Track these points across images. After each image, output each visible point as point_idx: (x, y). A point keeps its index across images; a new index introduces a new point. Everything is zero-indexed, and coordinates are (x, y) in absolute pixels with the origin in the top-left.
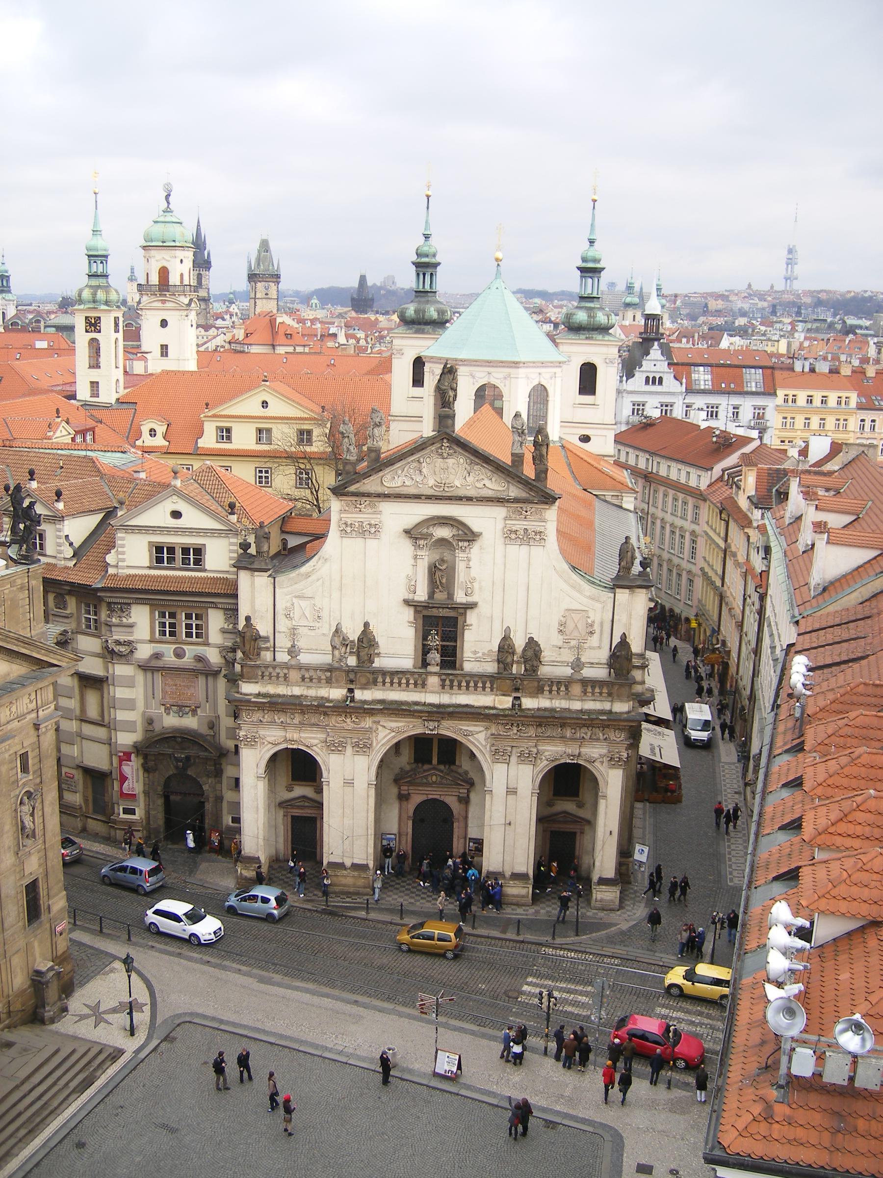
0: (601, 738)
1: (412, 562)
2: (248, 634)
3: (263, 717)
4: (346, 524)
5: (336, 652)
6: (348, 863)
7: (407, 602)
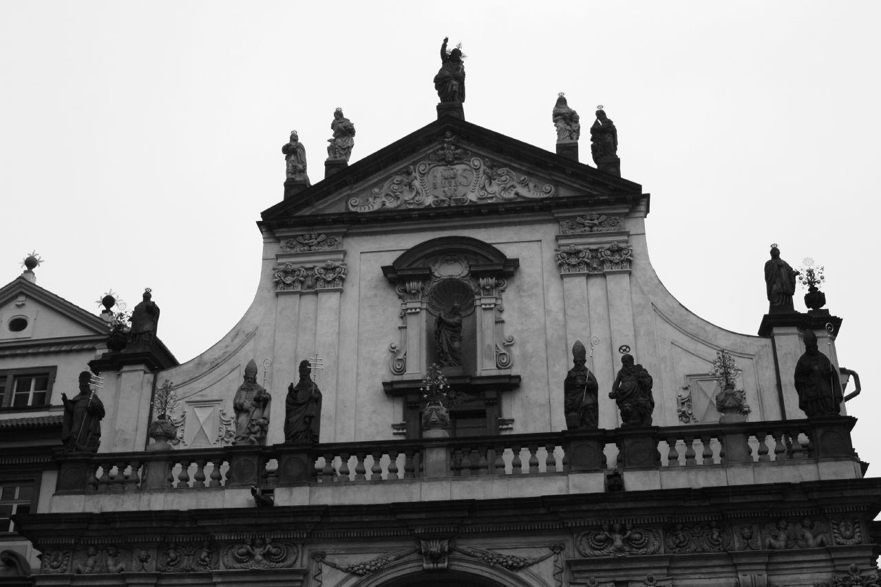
0: (811, 542)
3: (85, 565)
4: (286, 273)
5: (243, 419)
7: (392, 391)
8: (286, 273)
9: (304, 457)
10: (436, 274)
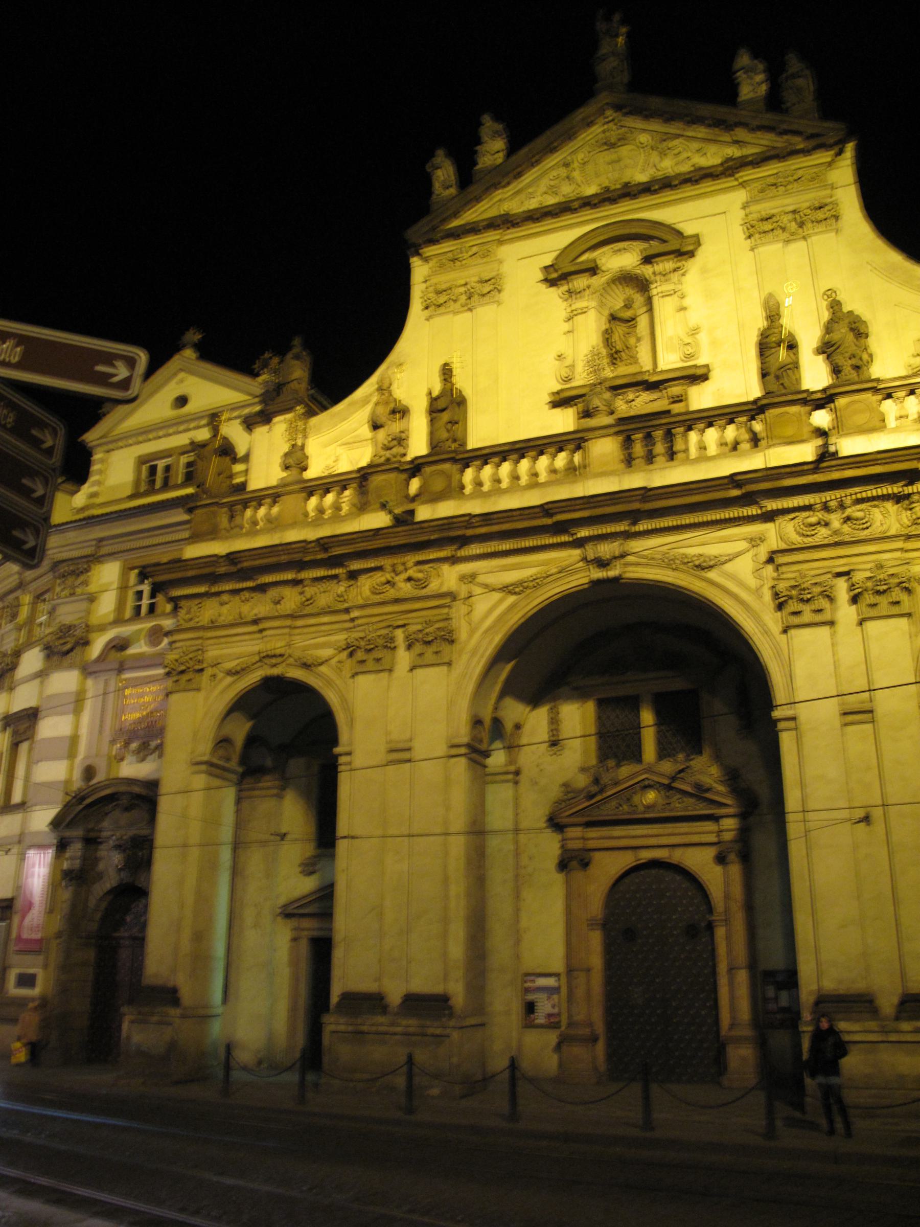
1: (566, 327)
2: (209, 448)
4: (439, 293)
6: (395, 995)
8: (439, 293)
9: (447, 466)
10: (604, 268)
